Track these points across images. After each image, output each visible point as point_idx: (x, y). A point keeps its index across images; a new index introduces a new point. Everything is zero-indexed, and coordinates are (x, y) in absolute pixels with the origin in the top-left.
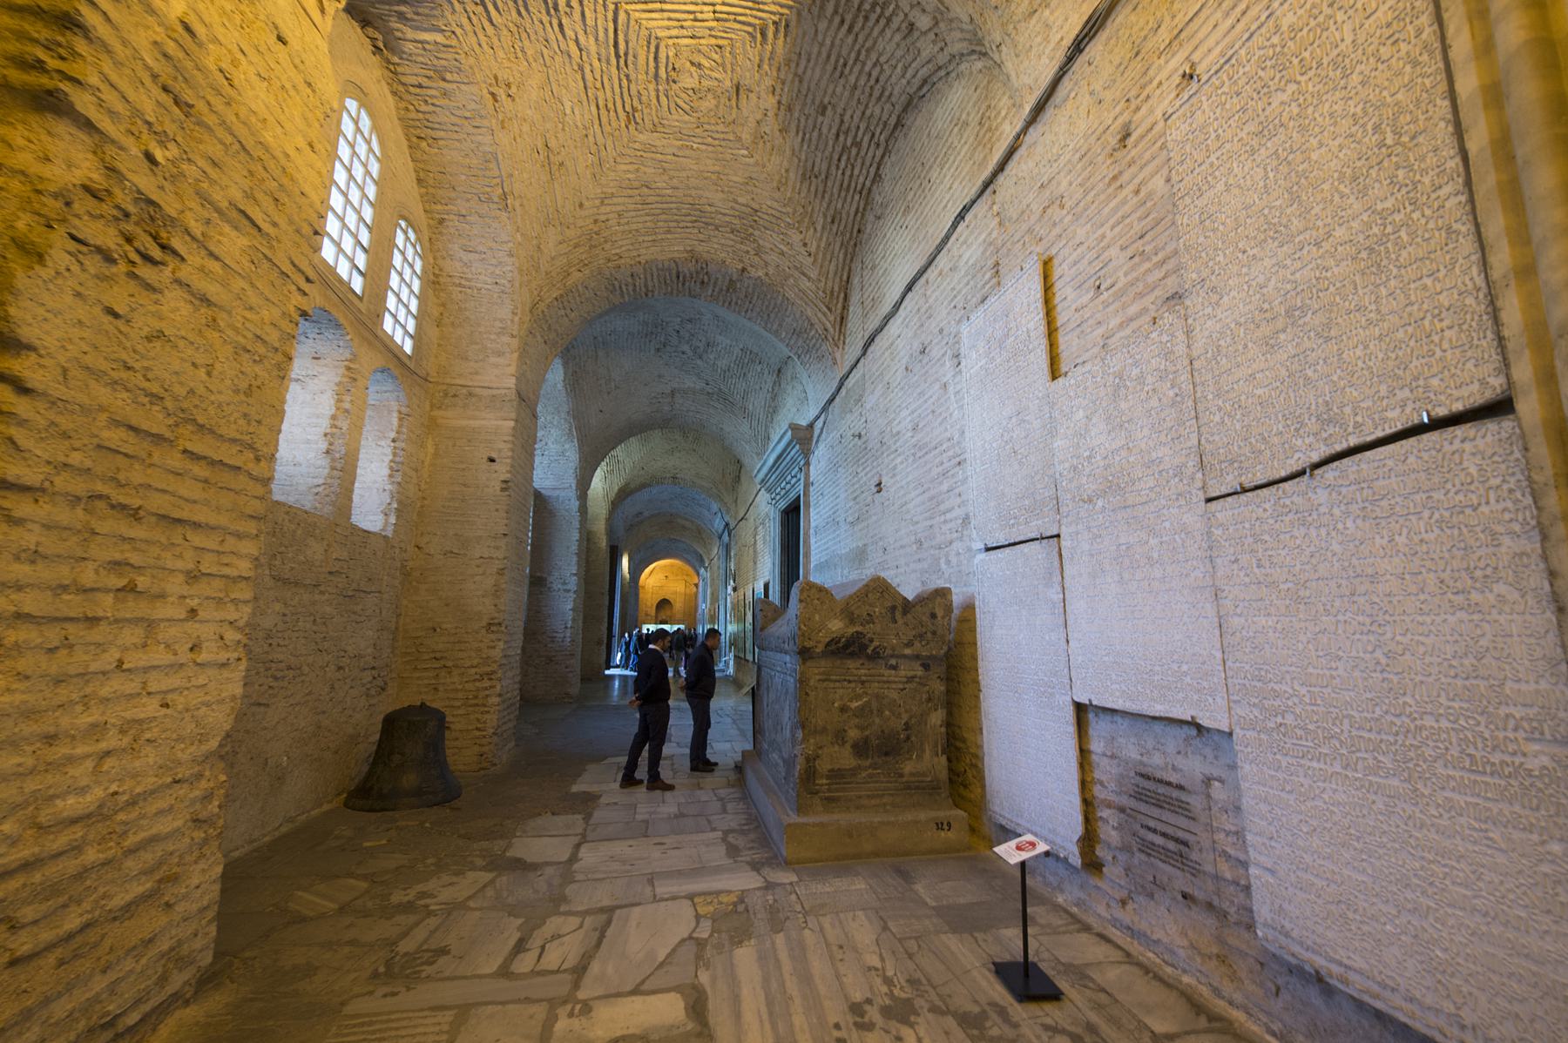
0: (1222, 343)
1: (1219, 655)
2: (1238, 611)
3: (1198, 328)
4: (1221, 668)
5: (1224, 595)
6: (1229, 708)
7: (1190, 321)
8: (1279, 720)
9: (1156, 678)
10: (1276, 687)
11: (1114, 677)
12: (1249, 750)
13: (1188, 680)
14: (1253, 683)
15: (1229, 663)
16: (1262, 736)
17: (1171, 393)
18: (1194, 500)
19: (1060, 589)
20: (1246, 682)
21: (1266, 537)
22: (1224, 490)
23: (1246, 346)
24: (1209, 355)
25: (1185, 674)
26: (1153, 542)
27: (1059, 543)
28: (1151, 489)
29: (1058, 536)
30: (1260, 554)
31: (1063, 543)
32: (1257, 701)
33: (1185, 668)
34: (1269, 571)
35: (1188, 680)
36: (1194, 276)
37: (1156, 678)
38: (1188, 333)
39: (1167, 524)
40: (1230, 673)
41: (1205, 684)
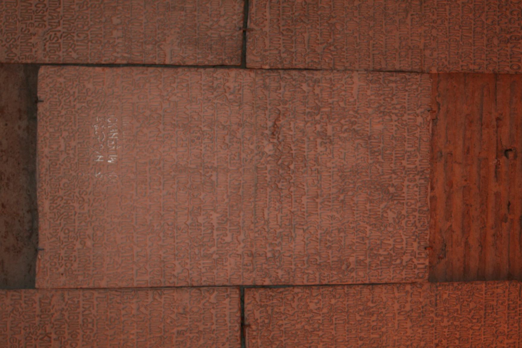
0: (374, 318)
1: (103, 284)
2: (142, 309)
3: (397, 295)
4: (91, 286)
5: (157, 297)
6: (57, 289)
7: (408, 287)
8: (53, 336)
9: (76, 205)
10: (80, 337)
11: (73, 144)
12: (24, 305)
13: (78, 246)
14: (80, 316)
15: (96, 294)
16: (38, 319)
17: (352, 259)
18: (246, 275)
19: (176, 60)
20: (81, 309)
21: (202, 342)
22: (248, 307)
23: (361, 339)
24: (370, 304)
25: (84, 244)
26: (215, 216)
27: (236, 67)
28: (267, 222)
29: (243, 65)
30: (188, 334)
31: (233, 73)
32: (66, 317)
33: (89, 243)
34: (174, 340)
35: (78, 246)
36: (445, 296)
37: (76, 205)
38: (400, 285)
39: (228, 239)
40: (88, 294)
41: (76, 265)
